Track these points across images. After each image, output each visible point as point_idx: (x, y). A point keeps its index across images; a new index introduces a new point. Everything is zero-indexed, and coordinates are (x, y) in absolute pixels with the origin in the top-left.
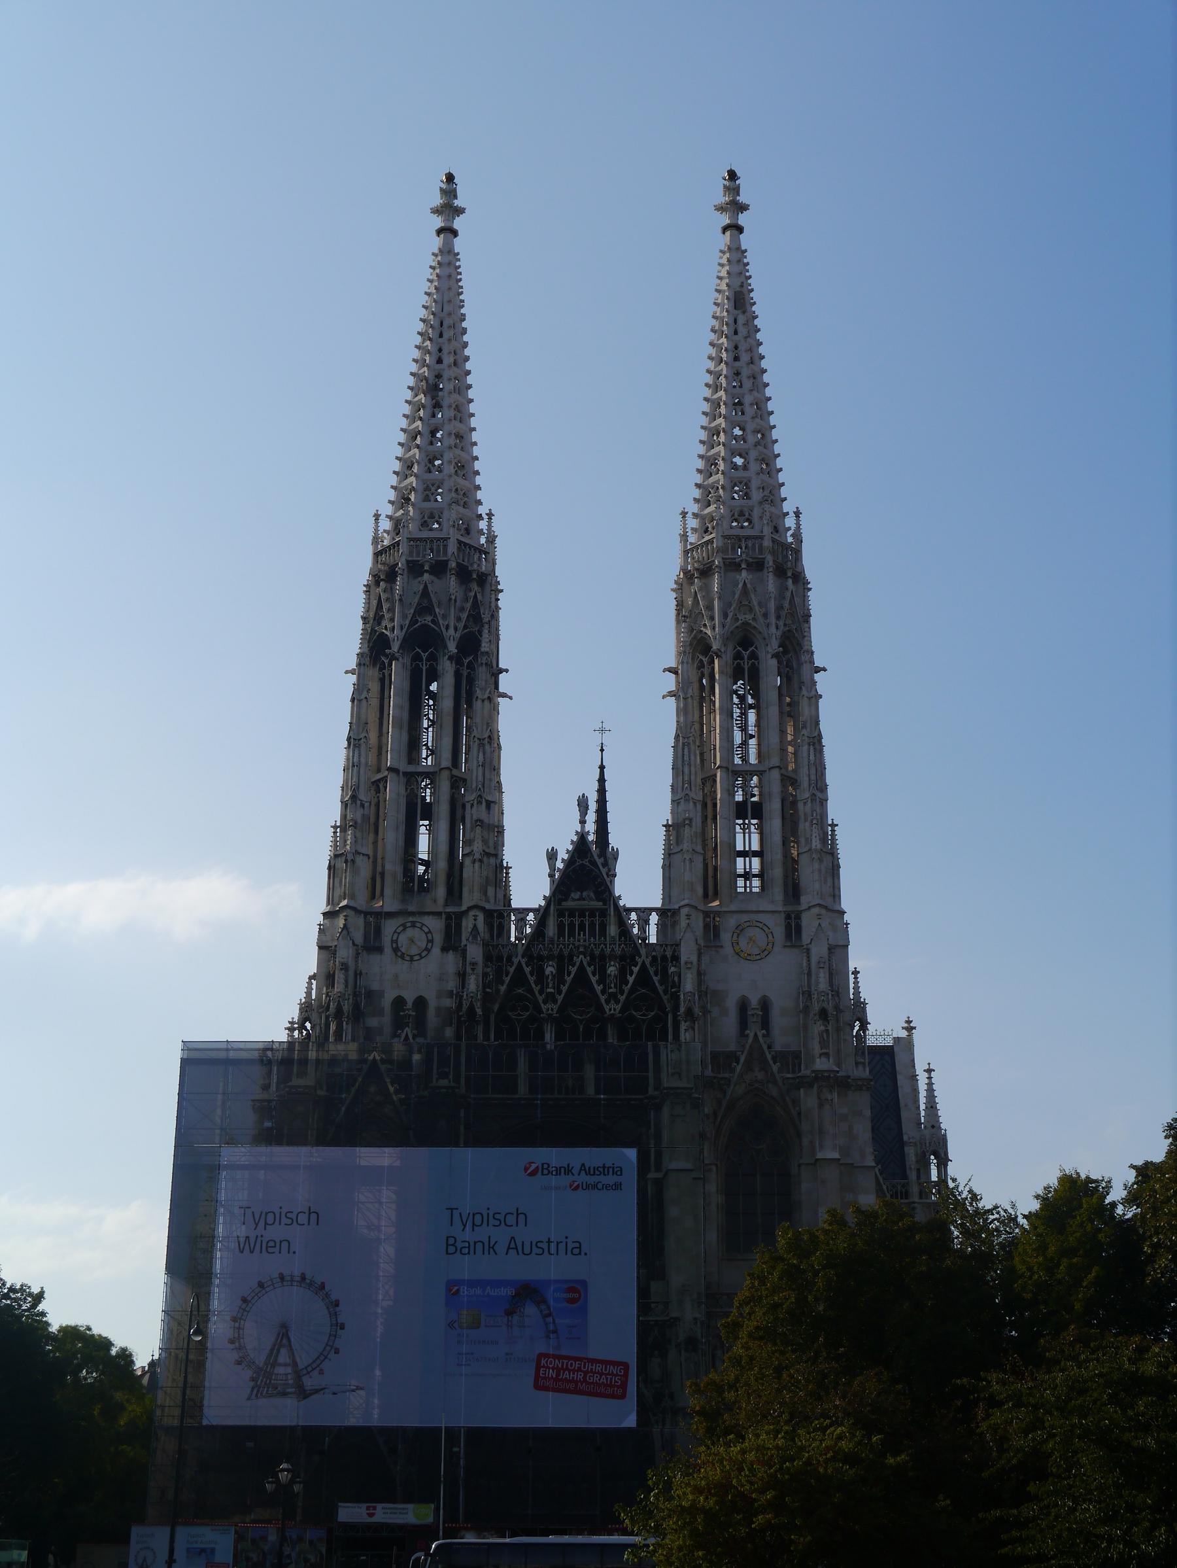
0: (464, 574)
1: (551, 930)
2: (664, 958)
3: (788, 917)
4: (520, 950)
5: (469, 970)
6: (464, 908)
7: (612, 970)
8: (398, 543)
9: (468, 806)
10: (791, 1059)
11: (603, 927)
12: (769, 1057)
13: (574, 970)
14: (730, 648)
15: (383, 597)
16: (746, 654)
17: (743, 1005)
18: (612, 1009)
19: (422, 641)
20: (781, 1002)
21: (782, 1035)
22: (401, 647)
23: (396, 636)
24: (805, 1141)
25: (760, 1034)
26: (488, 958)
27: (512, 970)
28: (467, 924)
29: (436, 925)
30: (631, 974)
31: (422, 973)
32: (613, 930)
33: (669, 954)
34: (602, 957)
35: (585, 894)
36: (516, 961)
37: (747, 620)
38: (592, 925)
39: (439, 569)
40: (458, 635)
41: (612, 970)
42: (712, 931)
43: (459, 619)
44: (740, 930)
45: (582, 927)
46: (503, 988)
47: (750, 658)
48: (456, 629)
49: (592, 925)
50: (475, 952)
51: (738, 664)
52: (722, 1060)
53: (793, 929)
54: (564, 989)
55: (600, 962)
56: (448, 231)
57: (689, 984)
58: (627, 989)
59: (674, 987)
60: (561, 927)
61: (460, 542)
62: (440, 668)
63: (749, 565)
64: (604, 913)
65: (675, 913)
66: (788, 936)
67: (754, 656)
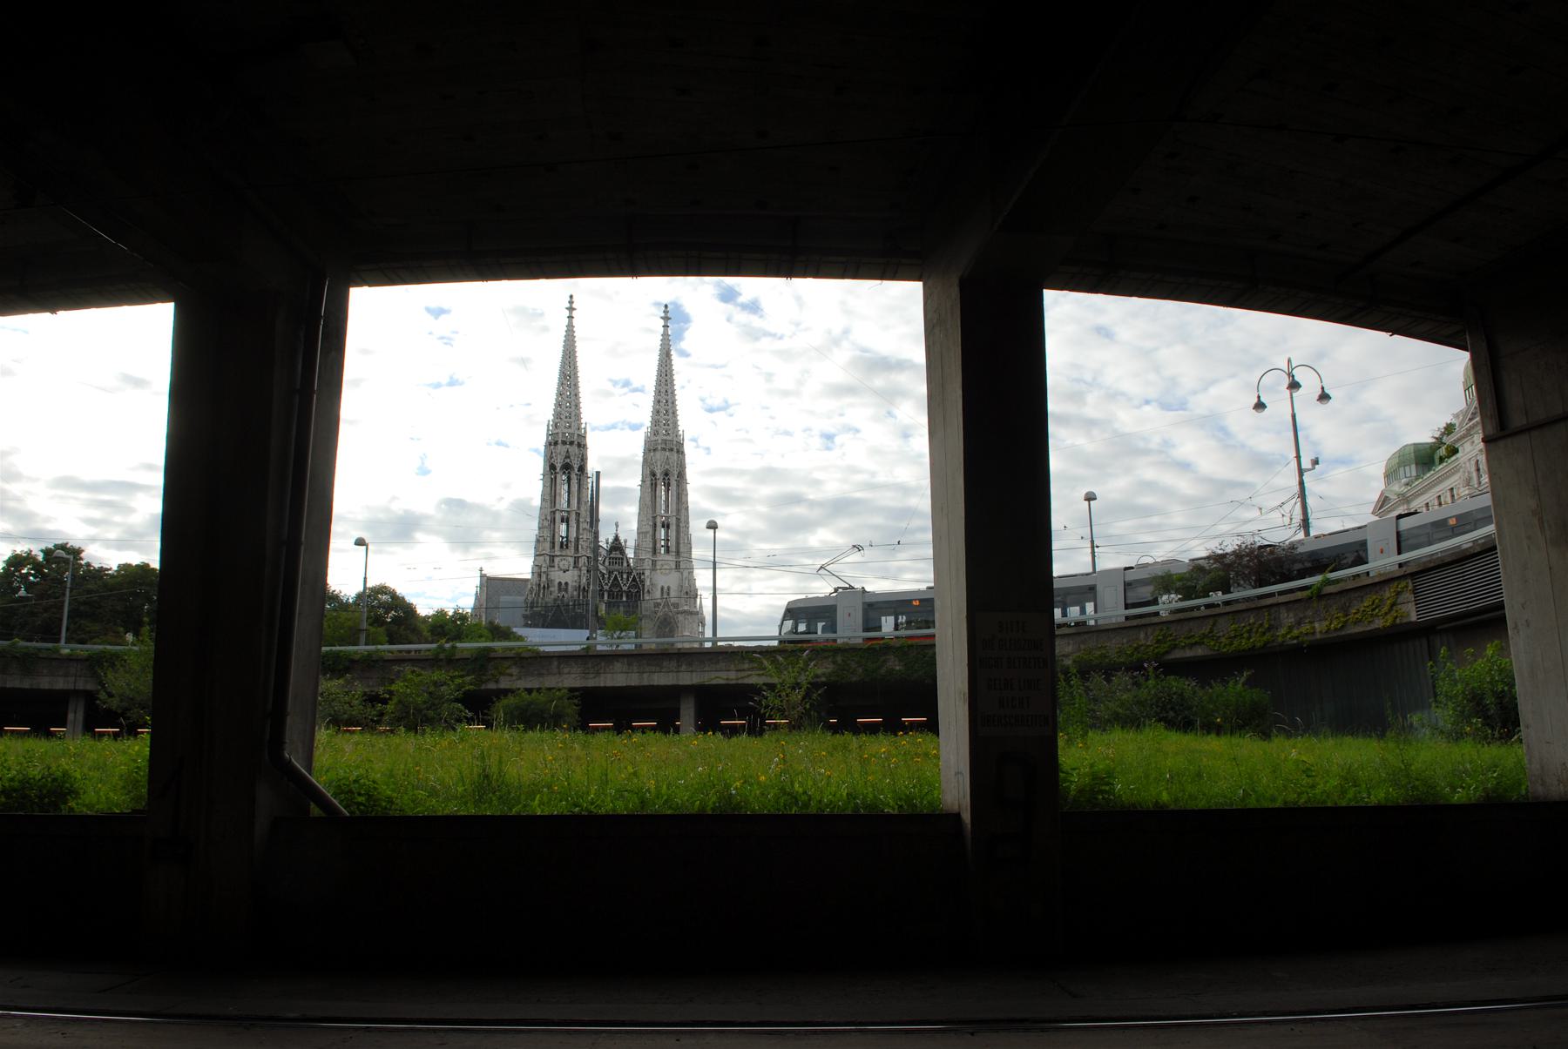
0: (579, 445)
10: (676, 605)
19: (567, 467)
20: (674, 588)
23: (558, 466)
28: (582, 561)
29: (571, 560)
31: (567, 576)
37: (664, 465)
39: (572, 443)
42: (654, 568)
50: (584, 569)
52: (657, 605)
53: (678, 567)
55: (621, 574)
56: (571, 317)
57: (647, 583)
59: (642, 582)
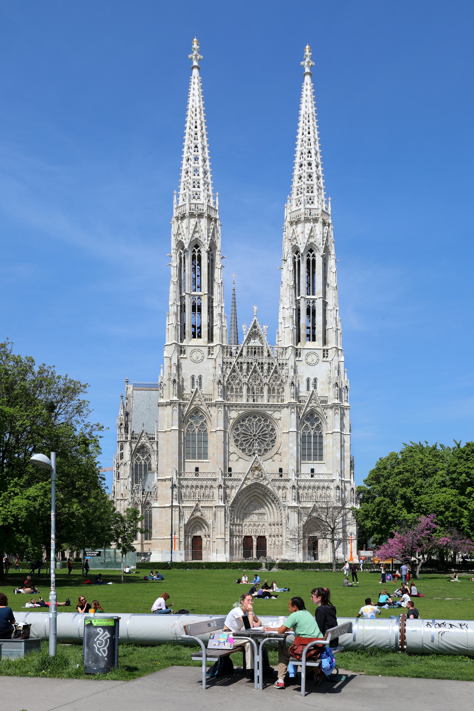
1: (244, 353)
2: (283, 364)
3: (324, 351)
4: (234, 360)
5: (217, 366)
6: (215, 345)
7: (266, 367)
8: (185, 204)
9: (214, 308)
11: (262, 352)
12: (317, 398)
13: (253, 367)
14: (306, 252)
15: (180, 226)
16: (311, 255)
17: (308, 380)
18: (266, 380)
19: (196, 245)
21: (321, 391)
22: (189, 247)
24: (329, 426)
25: (314, 390)
26: (223, 362)
27: (232, 367)
29: (206, 350)
30: (272, 369)
32: (265, 354)
33: (284, 362)
34: (262, 363)
35: (256, 341)
36: (233, 364)
38: (259, 351)
40: (209, 242)
41: (266, 367)
43: (208, 237)
44: (308, 355)
45: (255, 352)
46: (229, 373)
47: (312, 256)
48: (208, 240)
49: (259, 351)
50: (219, 361)
51: (308, 258)
54: (250, 373)
58: (271, 374)
60: (248, 352)
61: (208, 206)
62: (202, 255)
63: (313, 220)
64: (262, 347)
65: (286, 348)
66: (324, 357)
67: (314, 256)
